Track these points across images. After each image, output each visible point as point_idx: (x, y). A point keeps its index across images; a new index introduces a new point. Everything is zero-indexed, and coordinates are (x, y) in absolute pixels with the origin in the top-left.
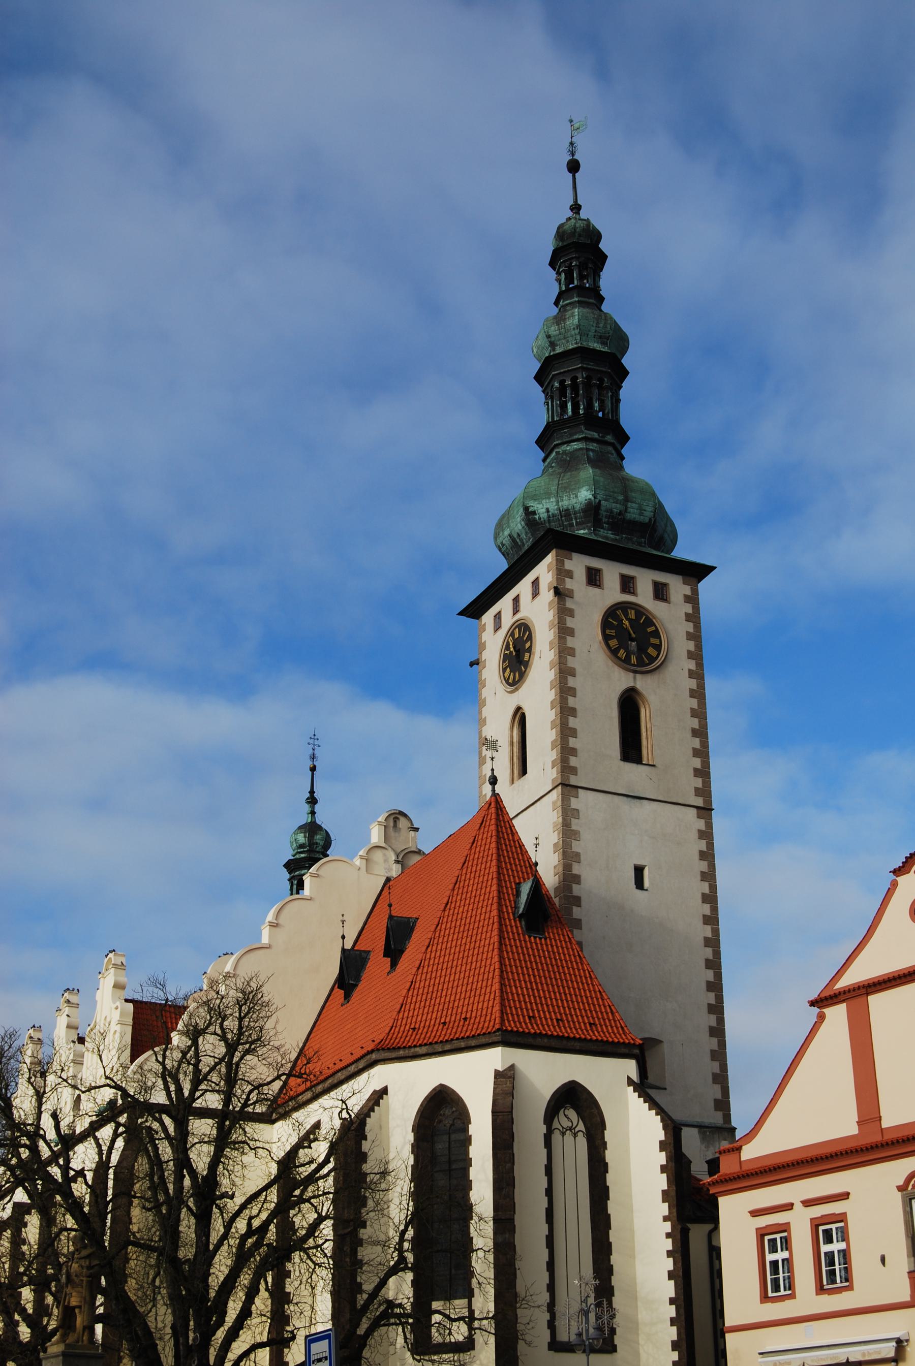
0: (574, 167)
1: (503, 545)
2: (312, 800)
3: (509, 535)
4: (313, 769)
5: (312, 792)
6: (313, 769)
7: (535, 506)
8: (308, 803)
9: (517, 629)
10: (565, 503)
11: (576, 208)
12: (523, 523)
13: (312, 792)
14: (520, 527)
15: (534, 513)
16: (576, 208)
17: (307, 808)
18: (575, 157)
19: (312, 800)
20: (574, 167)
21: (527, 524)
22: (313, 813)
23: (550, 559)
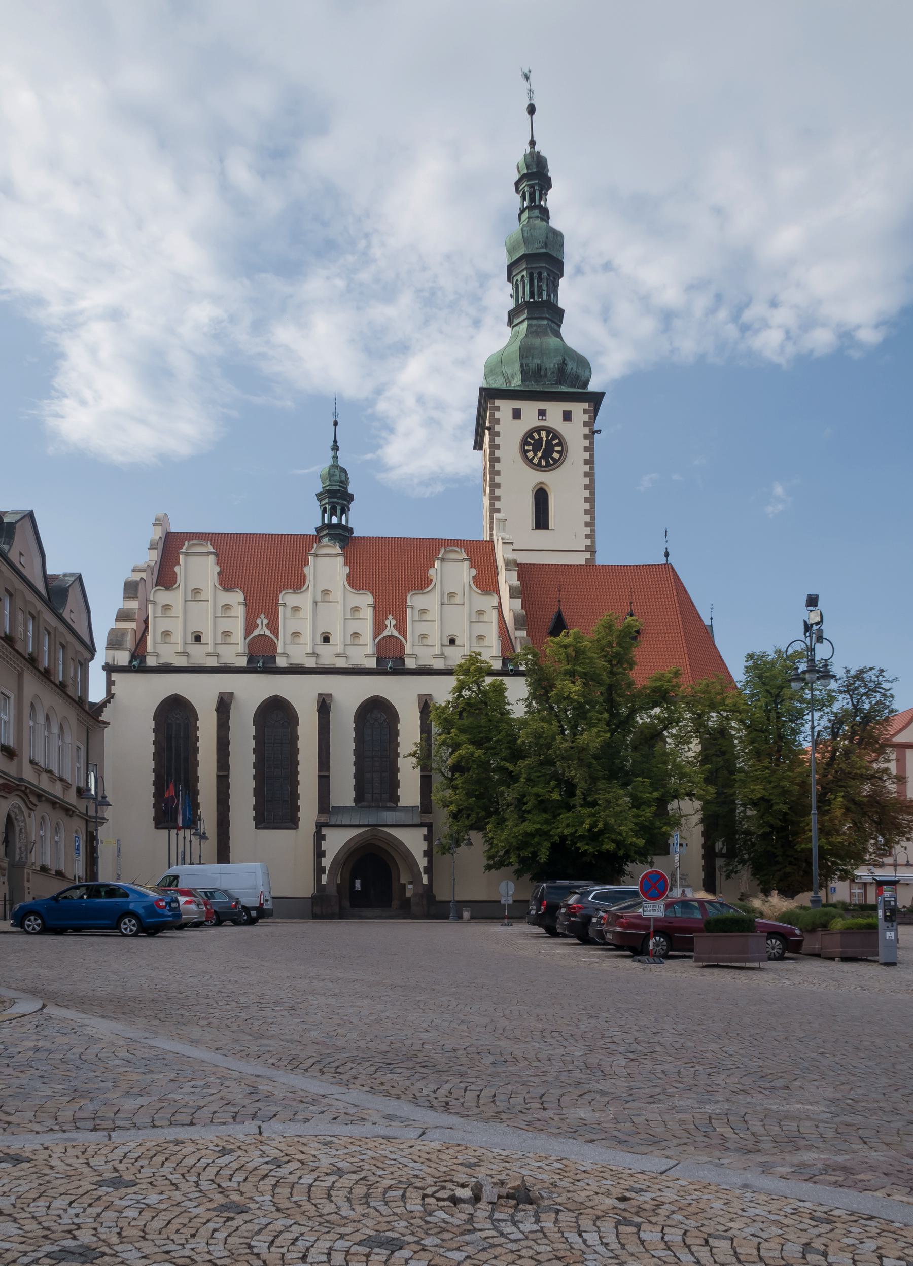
0: (531, 110)
1: (527, 365)
2: (335, 448)
3: (538, 365)
4: (336, 424)
5: (335, 441)
6: (336, 424)
7: (568, 361)
8: (332, 449)
9: (544, 432)
10: (580, 371)
11: (532, 143)
12: (556, 366)
13: (335, 441)
14: (552, 365)
15: (566, 365)
16: (532, 143)
17: (331, 453)
18: (532, 102)
19: (335, 448)
20: (531, 110)
21: (559, 369)
22: (335, 458)
23: (586, 405)
